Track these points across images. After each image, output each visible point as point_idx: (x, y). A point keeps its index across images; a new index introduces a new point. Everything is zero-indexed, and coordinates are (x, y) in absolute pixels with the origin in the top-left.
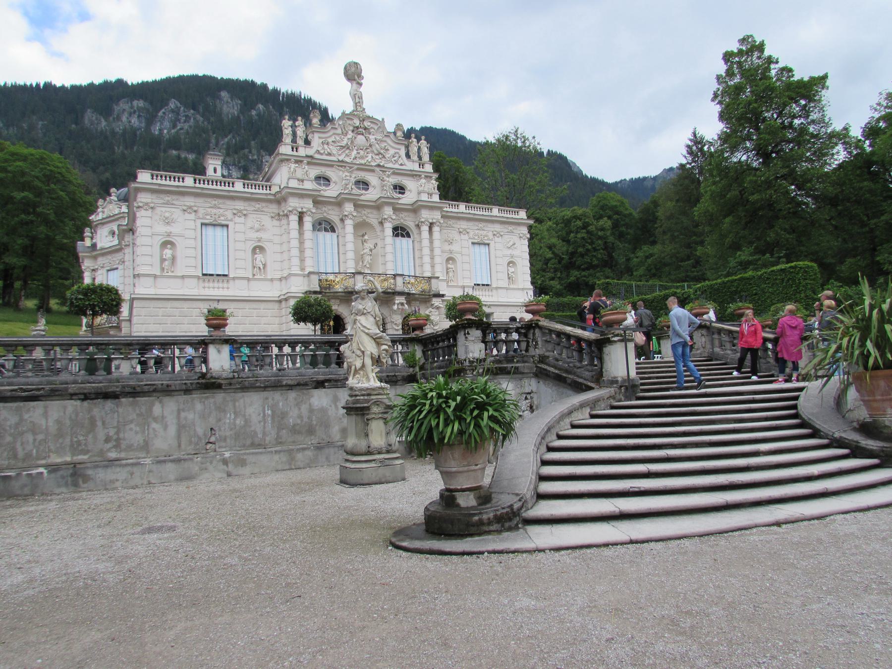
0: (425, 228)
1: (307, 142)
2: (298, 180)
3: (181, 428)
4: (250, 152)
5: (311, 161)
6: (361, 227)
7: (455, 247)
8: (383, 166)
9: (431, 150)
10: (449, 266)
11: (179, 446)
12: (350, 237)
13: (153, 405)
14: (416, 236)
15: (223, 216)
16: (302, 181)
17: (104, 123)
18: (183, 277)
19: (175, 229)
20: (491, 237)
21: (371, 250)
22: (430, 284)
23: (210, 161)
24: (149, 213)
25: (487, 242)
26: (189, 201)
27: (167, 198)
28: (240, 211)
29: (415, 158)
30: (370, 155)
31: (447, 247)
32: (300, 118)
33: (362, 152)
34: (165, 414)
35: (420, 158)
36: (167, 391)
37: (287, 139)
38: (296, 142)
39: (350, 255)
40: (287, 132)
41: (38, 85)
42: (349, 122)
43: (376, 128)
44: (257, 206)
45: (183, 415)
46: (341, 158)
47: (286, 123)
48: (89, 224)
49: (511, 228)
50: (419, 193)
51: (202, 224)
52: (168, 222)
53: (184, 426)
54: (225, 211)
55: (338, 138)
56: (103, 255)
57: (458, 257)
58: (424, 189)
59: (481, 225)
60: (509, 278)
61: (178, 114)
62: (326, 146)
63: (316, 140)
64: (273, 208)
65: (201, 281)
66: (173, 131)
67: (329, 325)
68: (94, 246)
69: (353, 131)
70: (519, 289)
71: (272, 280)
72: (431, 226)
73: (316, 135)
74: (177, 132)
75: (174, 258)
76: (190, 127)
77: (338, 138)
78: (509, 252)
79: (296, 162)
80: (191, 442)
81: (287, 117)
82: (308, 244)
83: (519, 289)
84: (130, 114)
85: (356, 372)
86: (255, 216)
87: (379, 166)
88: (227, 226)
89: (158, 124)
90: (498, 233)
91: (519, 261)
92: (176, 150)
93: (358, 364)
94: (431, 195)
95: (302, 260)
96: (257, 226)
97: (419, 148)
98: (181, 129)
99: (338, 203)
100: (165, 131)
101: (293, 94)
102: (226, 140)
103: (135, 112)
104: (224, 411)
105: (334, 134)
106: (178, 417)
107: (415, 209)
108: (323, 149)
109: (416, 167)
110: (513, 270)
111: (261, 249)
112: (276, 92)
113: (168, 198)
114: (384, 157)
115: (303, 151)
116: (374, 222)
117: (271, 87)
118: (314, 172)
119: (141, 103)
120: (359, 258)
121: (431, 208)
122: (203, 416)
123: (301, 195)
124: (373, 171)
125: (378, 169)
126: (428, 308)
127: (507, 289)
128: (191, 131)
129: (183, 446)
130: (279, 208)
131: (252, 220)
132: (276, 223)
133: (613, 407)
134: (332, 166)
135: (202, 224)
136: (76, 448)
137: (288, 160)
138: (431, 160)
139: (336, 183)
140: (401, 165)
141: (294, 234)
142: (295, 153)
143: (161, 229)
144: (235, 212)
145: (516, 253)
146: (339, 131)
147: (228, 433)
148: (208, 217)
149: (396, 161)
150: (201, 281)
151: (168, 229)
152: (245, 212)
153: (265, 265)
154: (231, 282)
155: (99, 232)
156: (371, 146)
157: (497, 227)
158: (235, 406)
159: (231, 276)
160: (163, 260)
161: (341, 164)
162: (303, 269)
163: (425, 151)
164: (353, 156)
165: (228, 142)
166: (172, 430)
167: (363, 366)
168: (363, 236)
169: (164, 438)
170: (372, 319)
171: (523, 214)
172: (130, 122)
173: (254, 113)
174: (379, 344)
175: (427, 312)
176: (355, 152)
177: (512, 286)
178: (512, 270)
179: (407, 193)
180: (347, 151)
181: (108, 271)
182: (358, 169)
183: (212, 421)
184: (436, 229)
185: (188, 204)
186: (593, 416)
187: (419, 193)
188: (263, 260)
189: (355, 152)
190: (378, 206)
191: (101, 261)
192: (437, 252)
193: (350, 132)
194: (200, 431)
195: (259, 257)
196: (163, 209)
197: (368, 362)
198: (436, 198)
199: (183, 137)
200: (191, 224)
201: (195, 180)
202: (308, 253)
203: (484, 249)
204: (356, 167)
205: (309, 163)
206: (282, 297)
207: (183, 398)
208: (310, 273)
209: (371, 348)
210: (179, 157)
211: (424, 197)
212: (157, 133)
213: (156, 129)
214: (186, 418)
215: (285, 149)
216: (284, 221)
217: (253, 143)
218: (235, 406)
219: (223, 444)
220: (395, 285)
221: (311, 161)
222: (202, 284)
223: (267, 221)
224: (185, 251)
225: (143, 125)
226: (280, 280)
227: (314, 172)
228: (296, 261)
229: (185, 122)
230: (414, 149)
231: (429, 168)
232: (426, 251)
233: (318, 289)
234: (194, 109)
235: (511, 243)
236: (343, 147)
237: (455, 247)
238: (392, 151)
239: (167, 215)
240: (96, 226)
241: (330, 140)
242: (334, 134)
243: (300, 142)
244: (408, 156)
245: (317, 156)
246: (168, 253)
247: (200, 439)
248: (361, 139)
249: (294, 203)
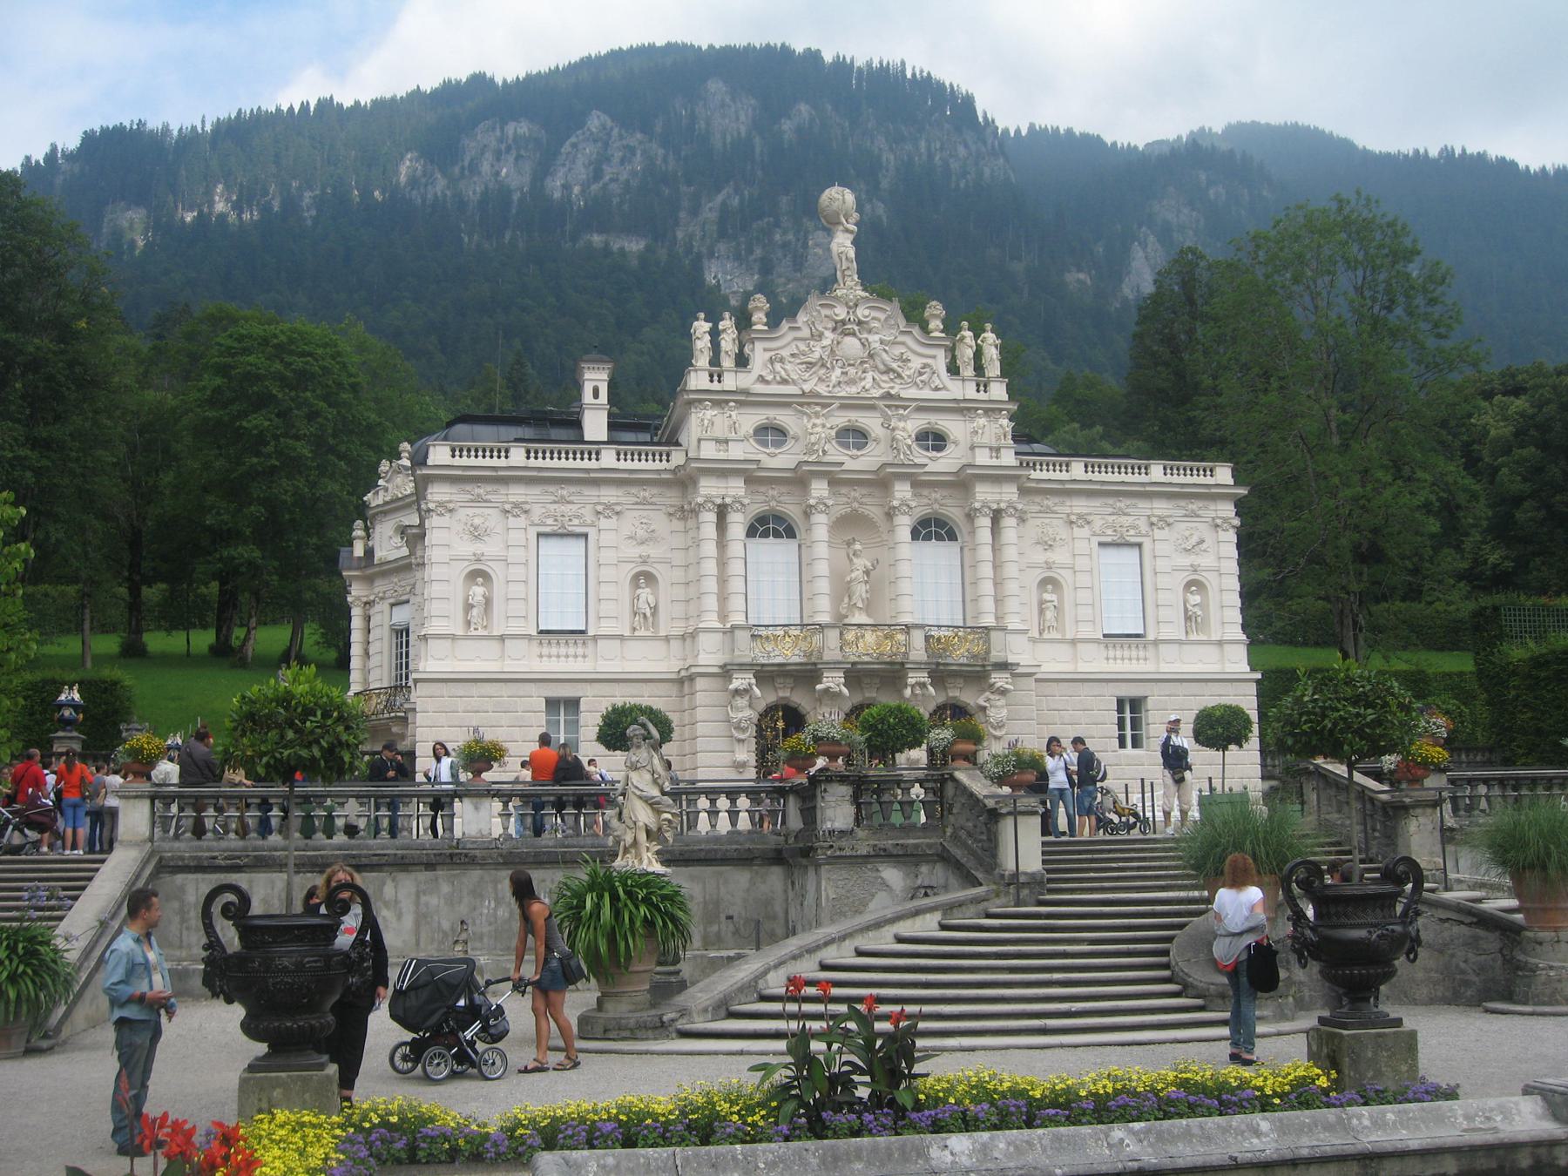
0: (984, 522)
1: (742, 361)
2: (718, 441)
3: (421, 918)
4: (777, 224)
5: (745, 399)
6: (850, 524)
7: (1059, 556)
8: (899, 398)
9: (1004, 351)
10: (1047, 596)
11: (418, 943)
12: (822, 550)
13: (384, 884)
14: (967, 538)
15: (578, 517)
16: (726, 441)
17: (441, 182)
18: (502, 638)
19: (491, 548)
20: (1144, 528)
21: (867, 573)
22: (988, 641)
23: (587, 376)
24: (445, 520)
25: (1133, 540)
26: (517, 493)
27: (477, 491)
28: (608, 506)
29: (968, 372)
30: (869, 376)
31: (1039, 556)
32: (727, 315)
33: (852, 371)
34: (400, 896)
35: (979, 369)
36: (402, 864)
37: (702, 361)
38: (719, 365)
39: (823, 586)
40: (702, 343)
41: (305, 107)
42: (825, 312)
43: (882, 316)
44: (642, 494)
45: (423, 899)
46: (807, 387)
47: (701, 327)
48: (362, 511)
49: (1194, 506)
50: (972, 448)
51: (539, 535)
52: (477, 534)
53: (425, 916)
54: (580, 506)
55: (802, 347)
56: (384, 574)
57: (1065, 576)
58: (984, 439)
59: (1122, 504)
60: (1188, 618)
61: (606, 145)
62: (778, 366)
63: (759, 355)
64: (672, 498)
65: (535, 643)
66: (594, 187)
67: (775, 729)
68: (369, 553)
69: (834, 330)
70: (1209, 643)
71: (667, 639)
72: (997, 517)
73: (759, 346)
74: (605, 185)
75: (488, 602)
76: (634, 173)
77: (802, 347)
78: (1185, 561)
79: (717, 404)
80: (433, 940)
81: (702, 315)
82: (736, 567)
83: (1209, 643)
84: (498, 155)
85: (626, 850)
86: (636, 513)
87: (888, 396)
88: (586, 536)
89: (561, 173)
90: (1161, 518)
91: (1211, 580)
92: (600, 232)
93: (629, 839)
94: (996, 450)
95: (723, 598)
96: (641, 533)
97: (978, 354)
98: (612, 180)
99: (798, 480)
100: (576, 190)
101: (884, 70)
102: (720, 198)
103: (509, 149)
104: (481, 896)
105: (796, 339)
106: (417, 903)
107: (962, 482)
108: (774, 372)
109: (970, 392)
110: (1197, 599)
112: (842, 67)
113: (481, 490)
114: (899, 376)
115: (730, 382)
116: (874, 512)
117: (828, 57)
118: (750, 420)
119: (523, 128)
120: (842, 589)
121: (997, 477)
122: (450, 901)
123: (723, 471)
124: (872, 408)
125: (881, 403)
126: (984, 691)
127: (1180, 642)
128: (634, 183)
129: (422, 945)
130: (684, 496)
131: (631, 522)
132: (677, 525)
133: (989, 916)
134: (787, 405)
135: (539, 535)
137: (700, 401)
138: (1003, 374)
139: (796, 439)
140: (937, 389)
141: (710, 548)
142: (716, 386)
143: (467, 548)
144: (600, 508)
145: (1206, 561)
146: (806, 333)
147: (485, 930)
148: (550, 521)
150: (535, 643)
151: (478, 547)
152: (618, 508)
153: (655, 610)
154: (590, 644)
155: (378, 528)
156: (871, 356)
157: (1161, 507)
158: (495, 889)
159: (591, 633)
160: (468, 607)
161: (806, 402)
162: (723, 616)
163: (992, 353)
164: (834, 379)
165: (724, 203)
166: (408, 921)
167: (635, 843)
168: (849, 544)
170: (648, 777)
171: (1223, 474)
172: (498, 173)
173: (787, 125)
174: (658, 812)
175: (981, 702)
176: (838, 371)
177: (1193, 637)
179: (950, 449)
180: (823, 371)
181: (392, 605)
182: (843, 407)
183: (463, 910)
184: (1009, 522)
185: (512, 499)
186: (943, 927)
187: (972, 448)
188: (651, 599)
189: (838, 371)
190: (881, 482)
191: (381, 586)
192: (1011, 570)
193: (828, 334)
194: (446, 925)
195: (645, 593)
196: (470, 512)
197: (642, 837)
198: (1008, 458)
199: (615, 201)
200: (516, 537)
201: (528, 452)
202: (736, 585)
203: (1131, 556)
204: (837, 403)
205: (740, 404)
206: (683, 673)
207: (424, 876)
208: (734, 628)
209: (644, 816)
210: (606, 251)
211: (983, 458)
212: (557, 195)
213: (555, 186)
214: (427, 905)
215: (697, 380)
216: (691, 523)
217: (784, 201)
218: (495, 889)
219: (478, 945)
220: (908, 645)
221: (745, 399)
222: (535, 648)
223: (660, 522)
225: (527, 179)
226: (683, 637)
227: (750, 420)
228: (711, 603)
229: (622, 162)
231: (998, 391)
232: (986, 570)
234: (643, 132)
235: (1194, 540)
236: (810, 365)
237: (1059, 556)
238: (916, 363)
239: (477, 521)
240: (374, 515)
241: (785, 353)
242: (796, 339)
243: (727, 362)
244: (953, 369)
245: (760, 388)
246: (478, 591)
247: (445, 934)
248: (851, 345)
249: (709, 488)
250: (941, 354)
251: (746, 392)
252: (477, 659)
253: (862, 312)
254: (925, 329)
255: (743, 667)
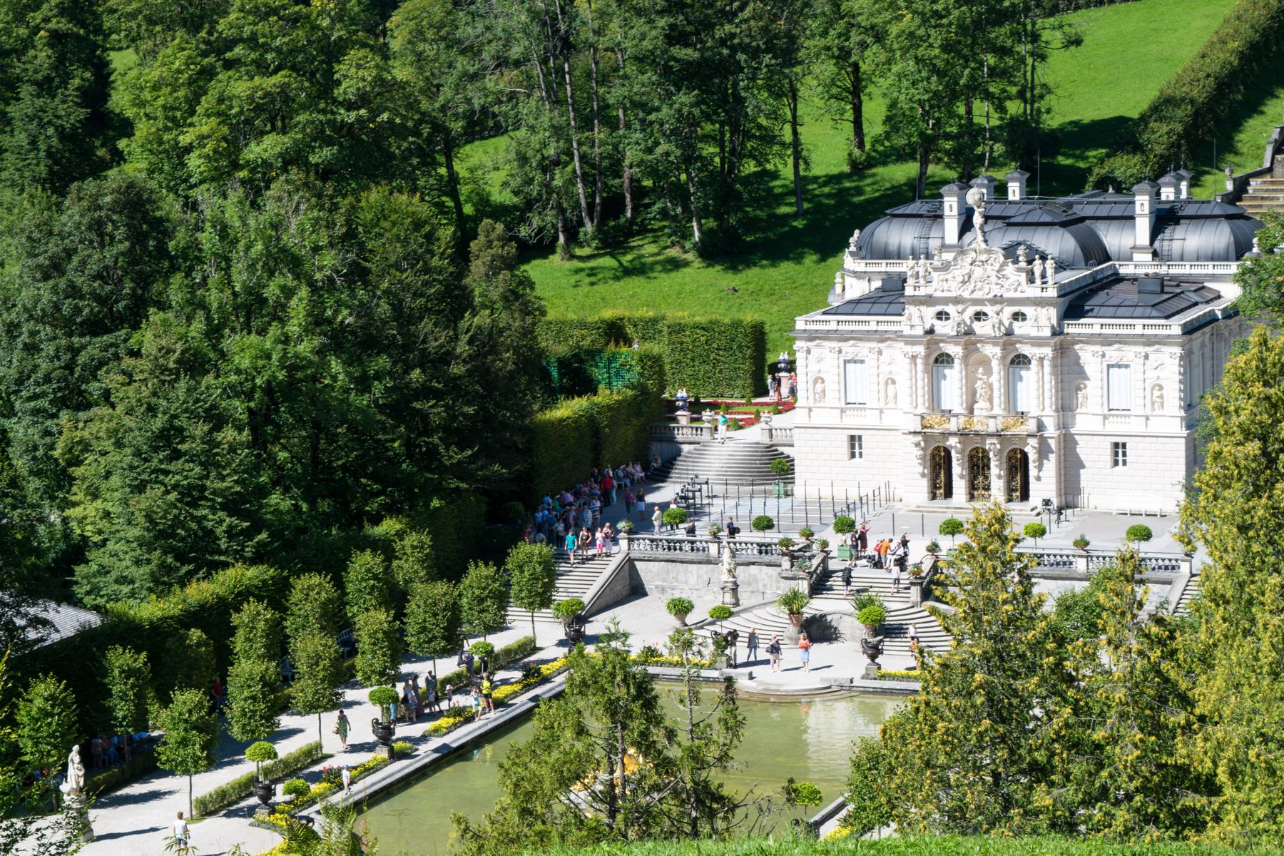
3: (699, 576)
5: (929, 300)
29: (1038, 281)
33: (979, 285)
46: (959, 293)
60: (1153, 403)
72: (1041, 359)
111: (894, 382)
115: (923, 292)
136: (664, 580)
142: (917, 293)
143: (813, 367)
149: (1016, 290)
161: (957, 301)
169: (693, 581)
178: (1156, 393)
195: (890, 387)
221: (929, 300)
224: (832, 385)
230: (1037, 273)
233: (919, 429)
241: (948, 277)
245: (938, 294)
246: (819, 386)
248: (978, 272)
250: (1024, 275)
251: (931, 296)
252: (819, 417)
253: (984, 257)
254: (1016, 261)
255: (915, 433)
